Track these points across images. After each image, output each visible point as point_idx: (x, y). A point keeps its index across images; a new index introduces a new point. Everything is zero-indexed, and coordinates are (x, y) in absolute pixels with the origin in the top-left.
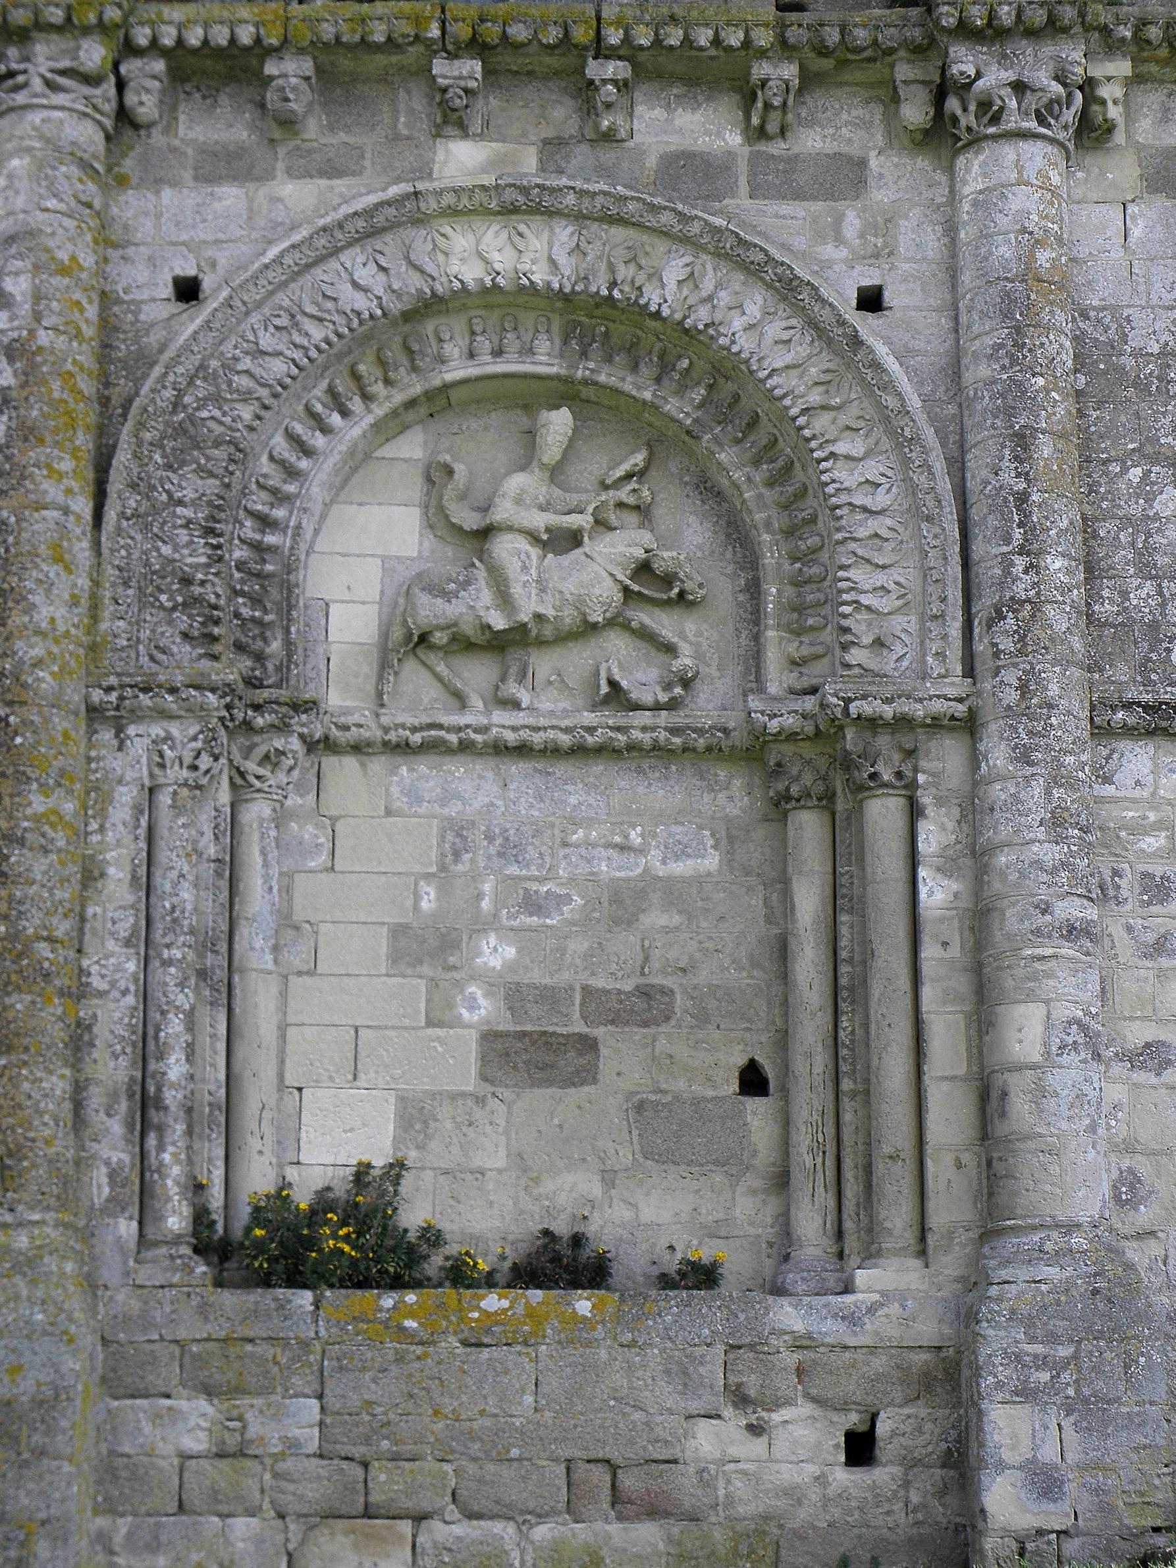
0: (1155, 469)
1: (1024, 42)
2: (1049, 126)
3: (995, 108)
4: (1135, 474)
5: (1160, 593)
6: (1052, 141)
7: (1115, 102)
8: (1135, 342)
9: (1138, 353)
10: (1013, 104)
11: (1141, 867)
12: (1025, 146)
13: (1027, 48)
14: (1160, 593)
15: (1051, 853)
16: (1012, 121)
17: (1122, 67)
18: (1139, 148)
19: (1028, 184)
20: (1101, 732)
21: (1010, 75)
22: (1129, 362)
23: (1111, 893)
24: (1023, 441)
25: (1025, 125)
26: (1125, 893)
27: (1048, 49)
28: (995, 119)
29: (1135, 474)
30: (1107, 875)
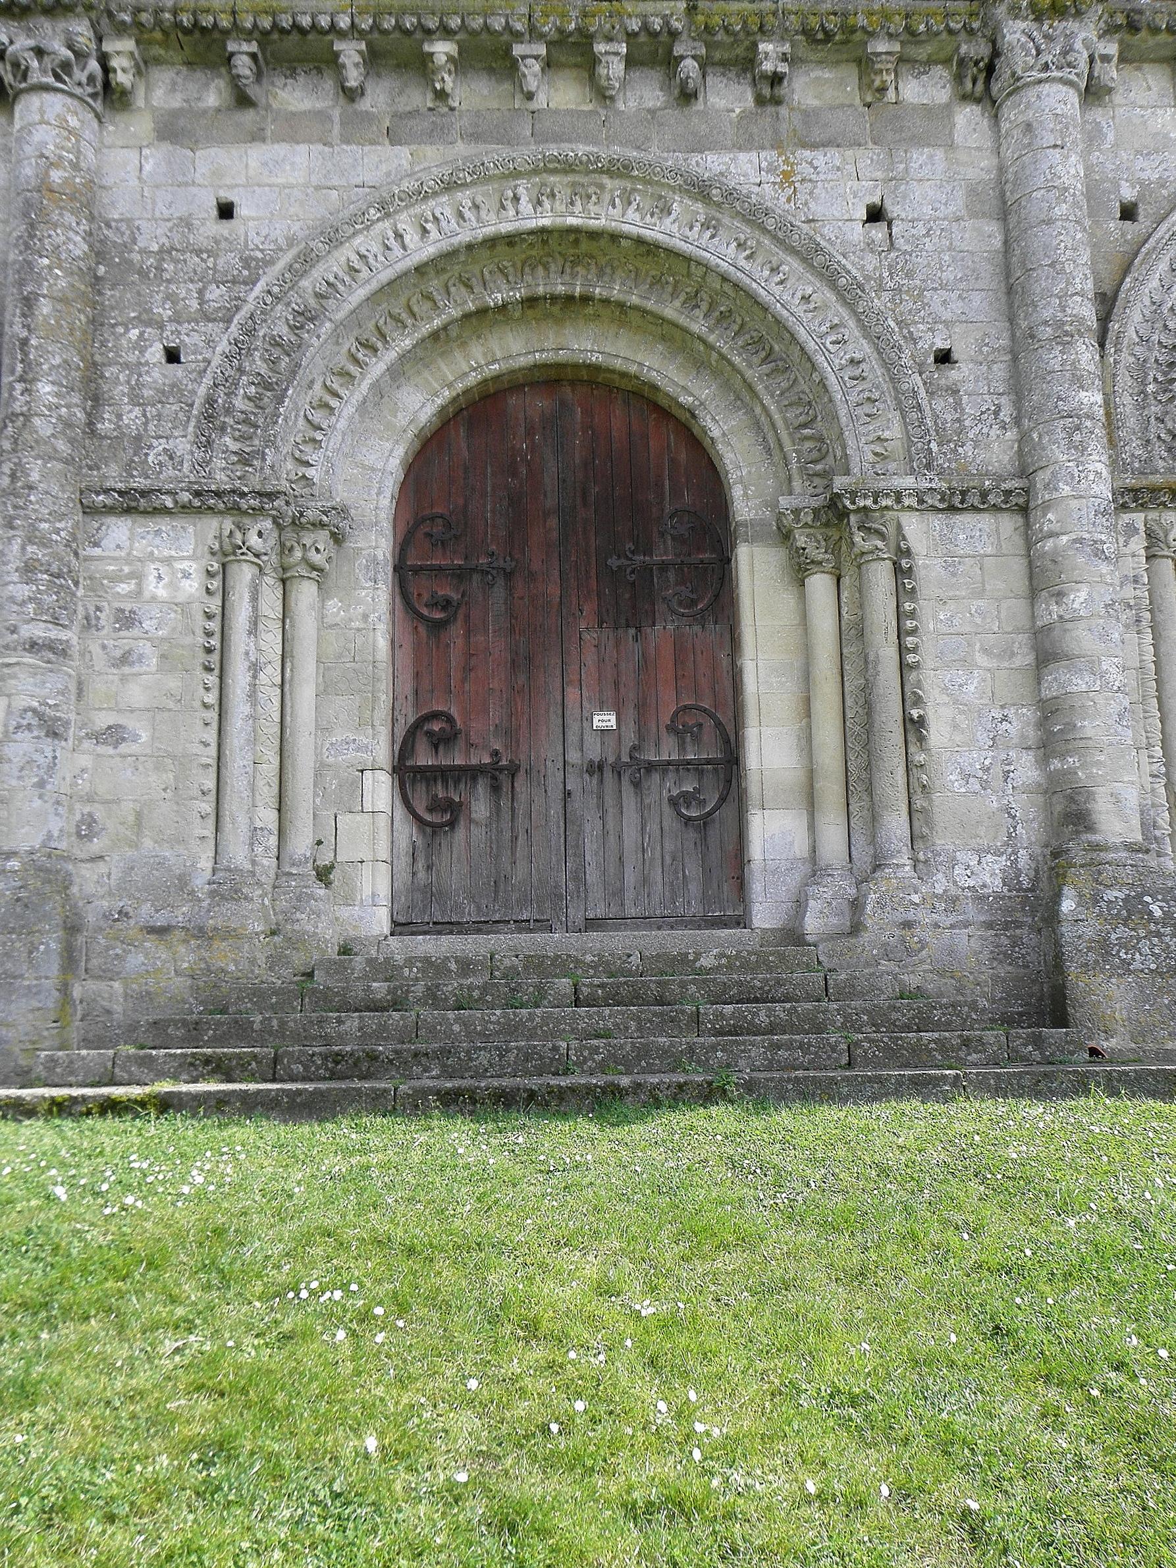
0: (148, 330)
1: (43, 18)
2: (64, 83)
3: (23, 67)
4: (134, 333)
5: (144, 415)
6: (71, 95)
7: (124, 70)
8: (141, 243)
9: (144, 251)
10: (35, 64)
11: (116, 605)
12: (48, 97)
13: (46, 24)
14: (144, 415)
15: (23, 591)
16: (35, 77)
17: (128, 44)
18: (154, 109)
19: (49, 124)
20: (90, 511)
21: (31, 43)
22: (136, 257)
23: (93, 622)
24: (29, 303)
25: (44, 80)
26: (102, 622)
27: (61, 25)
28: (25, 77)
29: (134, 333)
30: (92, 609)
